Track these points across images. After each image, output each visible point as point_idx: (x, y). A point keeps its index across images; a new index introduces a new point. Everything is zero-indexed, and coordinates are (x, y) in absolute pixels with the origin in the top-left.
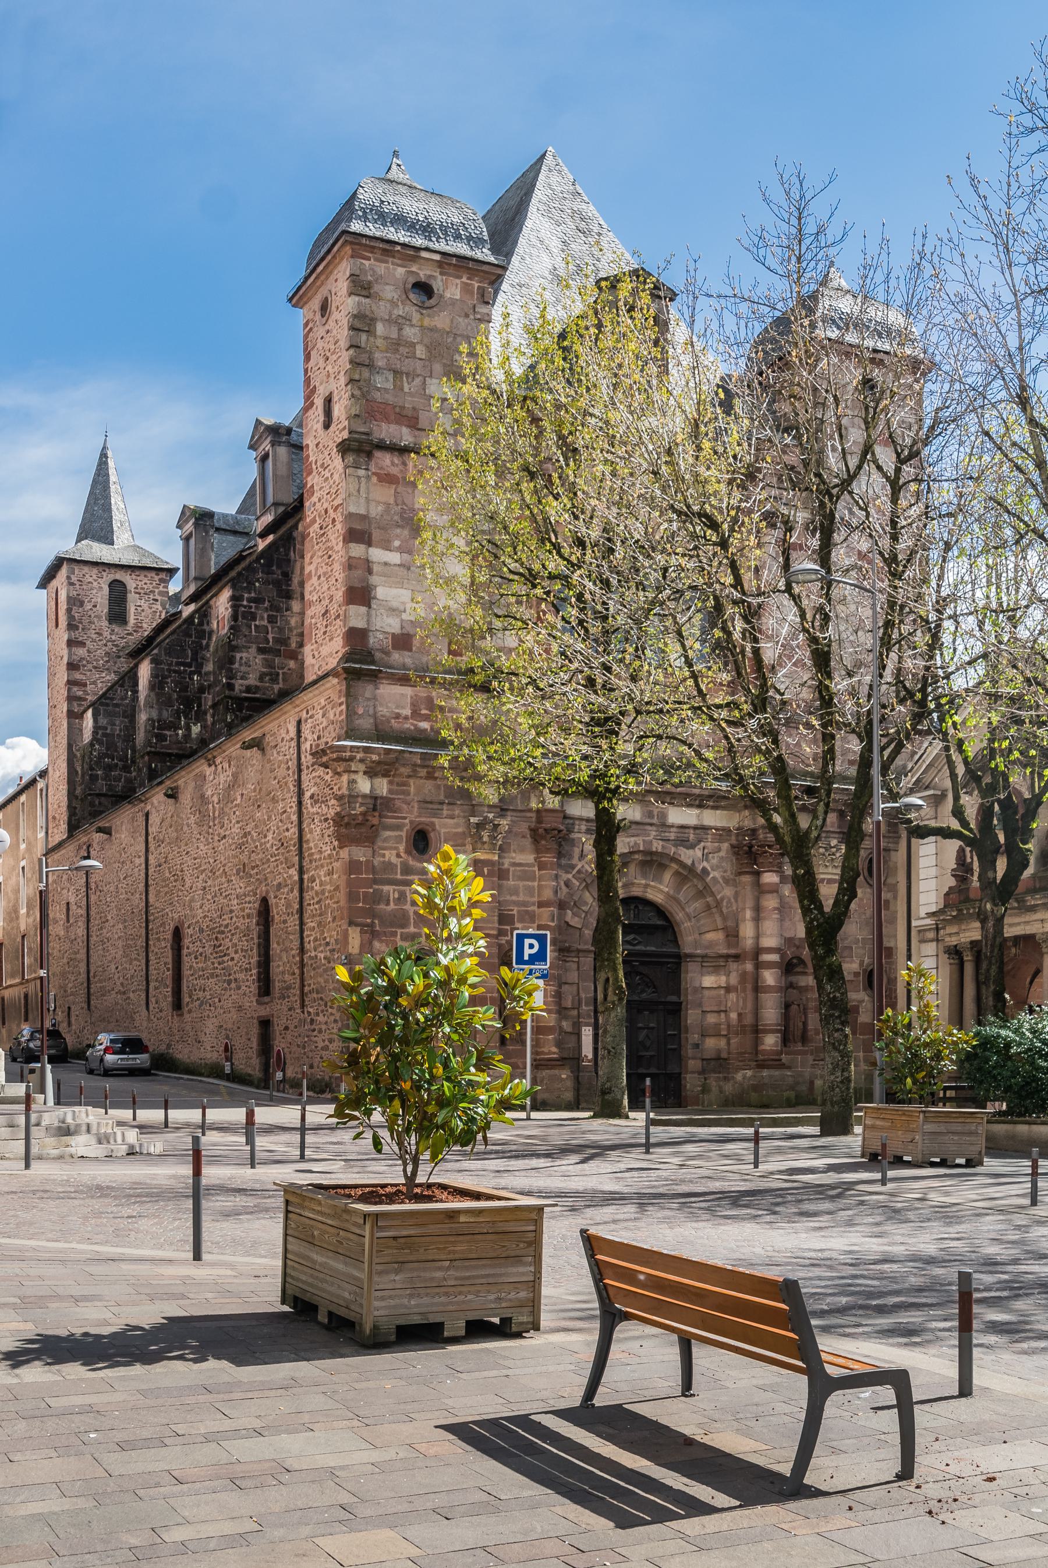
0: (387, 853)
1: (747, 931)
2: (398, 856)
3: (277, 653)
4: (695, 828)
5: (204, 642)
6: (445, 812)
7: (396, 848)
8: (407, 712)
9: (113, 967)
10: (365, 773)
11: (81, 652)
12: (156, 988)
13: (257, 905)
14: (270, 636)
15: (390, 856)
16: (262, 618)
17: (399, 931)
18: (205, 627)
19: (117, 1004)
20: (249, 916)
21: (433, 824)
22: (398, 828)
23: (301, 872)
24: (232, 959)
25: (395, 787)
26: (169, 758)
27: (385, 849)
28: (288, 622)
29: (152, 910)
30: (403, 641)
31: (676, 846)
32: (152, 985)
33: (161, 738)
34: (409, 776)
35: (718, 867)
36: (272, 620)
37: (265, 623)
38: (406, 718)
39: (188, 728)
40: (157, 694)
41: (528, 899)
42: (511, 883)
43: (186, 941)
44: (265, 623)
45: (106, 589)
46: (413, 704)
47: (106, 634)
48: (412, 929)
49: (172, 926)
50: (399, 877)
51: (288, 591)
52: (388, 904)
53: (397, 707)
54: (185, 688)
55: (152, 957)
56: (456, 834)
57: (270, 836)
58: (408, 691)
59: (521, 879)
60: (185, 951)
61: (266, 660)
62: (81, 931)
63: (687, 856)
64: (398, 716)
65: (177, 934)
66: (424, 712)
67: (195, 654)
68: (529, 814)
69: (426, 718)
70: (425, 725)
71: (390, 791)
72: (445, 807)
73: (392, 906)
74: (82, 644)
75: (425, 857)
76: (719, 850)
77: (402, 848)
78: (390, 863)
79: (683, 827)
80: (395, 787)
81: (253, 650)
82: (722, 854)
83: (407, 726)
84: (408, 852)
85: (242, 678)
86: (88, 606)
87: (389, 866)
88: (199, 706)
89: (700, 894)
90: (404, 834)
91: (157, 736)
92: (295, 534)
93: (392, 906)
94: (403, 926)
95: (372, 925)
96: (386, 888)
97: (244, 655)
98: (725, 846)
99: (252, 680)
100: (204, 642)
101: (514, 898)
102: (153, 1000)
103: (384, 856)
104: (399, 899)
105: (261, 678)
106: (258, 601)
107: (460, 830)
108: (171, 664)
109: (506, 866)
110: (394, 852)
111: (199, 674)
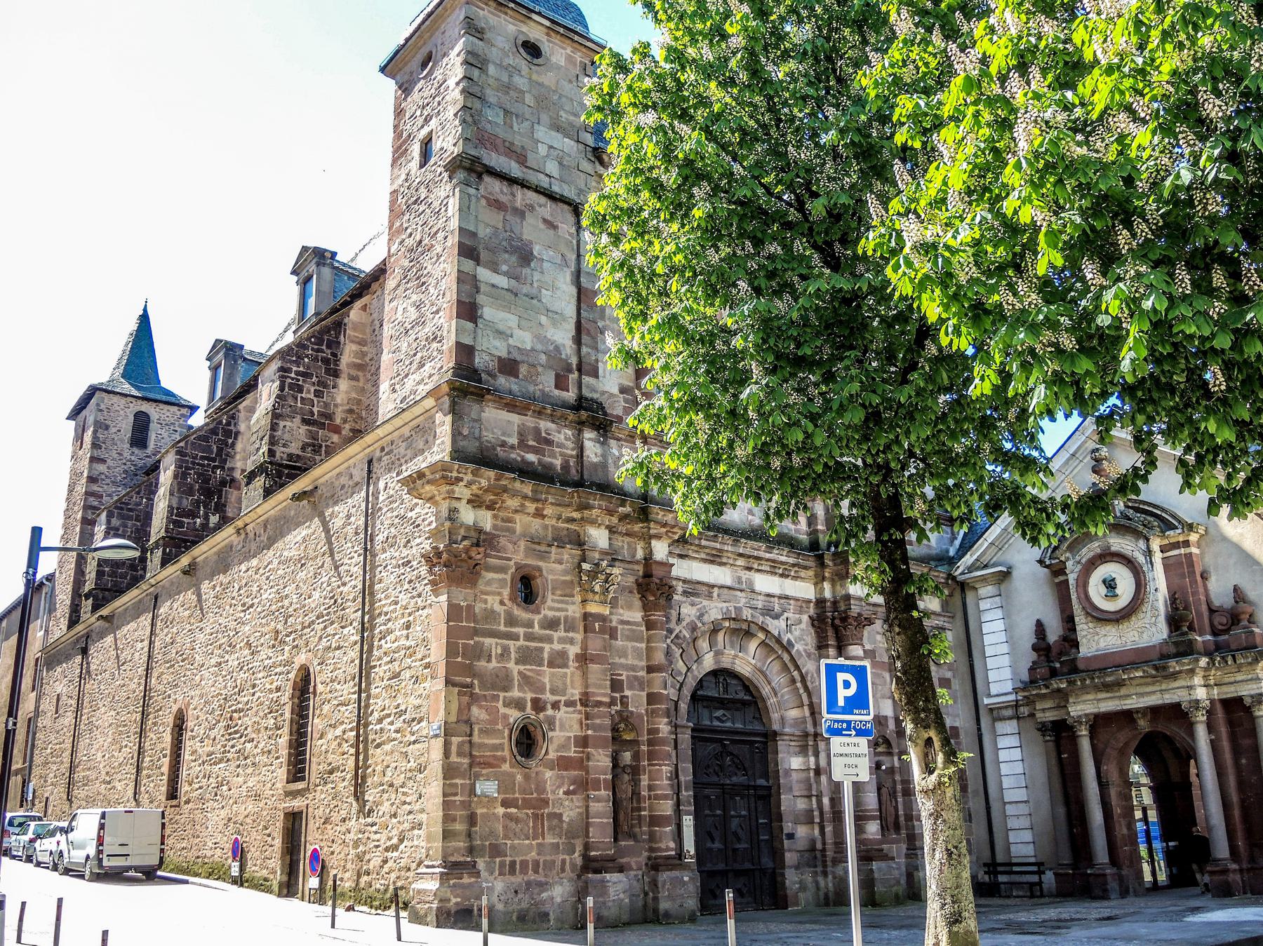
0: (489, 598)
4: (780, 597)
7: (499, 594)
8: (513, 440)
9: (100, 754)
11: (101, 468)
14: (315, 410)
15: (493, 602)
16: (309, 392)
17: (502, 695)
18: (232, 428)
20: (278, 689)
22: (502, 570)
25: (499, 523)
27: (487, 593)
28: (333, 398)
30: (509, 366)
31: (763, 615)
33: (178, 524)
34: (516, 511)
35: (801, 639)
36: (318, 394)
37: (312, 396)
38: (512, 447)
39: (207, 518)
40: (179, 483)
41: (636, 662)
42: (619, 643)
43: (190, 724)
44: (312, 396)
45: (131, 418)
46: (520, 434)
47: (127, 454)
48: (516, 693)
49: (175, 708)
50: (502, 628)
51: (336, 371)
52: (489, 661)
53: (504, 434)
54: (206, 481)
56: (564, 582)
57: (316, 595)
58: (515, 418)
59: (629, 639)
61: (310, 431)
62: (68, 719)
63: (776, 626)
64: (503, 444)
66: (531, 443)
67: (220, 450)
68: (636, 567)
69: (535, 451)
70: (531, 457)
71: (495, 527)
72: (553, 549)
73: (494, 664)
74: (103, 461)
75: (532, 607)
76: (800, 622)
77: (506, 592)
78: (493, 611)
79: (768, 595)
80: (499, 523)
81: (298, 419)
82: (803, 626)
84: (513, 599)
85: (284, 446)
87: (490, 615)
88: (220, 497)
90: (508, 577)
91: (175, 522)
92: (346, 321)
93: (494, 664)
94: (505, 689)
95: (471, 686)
96: (488, 641)
97: (288, 424)
98: (805, 618)
99: (294, 449)
101: (623, 661)
103: (486, 602)
104: (502, 655)
105: (303, 448)
106: (306, 375)
107: (568, 578)
108: (195, 458)
109: (614, 624)
110: (498, 598)
111: (223, 468)
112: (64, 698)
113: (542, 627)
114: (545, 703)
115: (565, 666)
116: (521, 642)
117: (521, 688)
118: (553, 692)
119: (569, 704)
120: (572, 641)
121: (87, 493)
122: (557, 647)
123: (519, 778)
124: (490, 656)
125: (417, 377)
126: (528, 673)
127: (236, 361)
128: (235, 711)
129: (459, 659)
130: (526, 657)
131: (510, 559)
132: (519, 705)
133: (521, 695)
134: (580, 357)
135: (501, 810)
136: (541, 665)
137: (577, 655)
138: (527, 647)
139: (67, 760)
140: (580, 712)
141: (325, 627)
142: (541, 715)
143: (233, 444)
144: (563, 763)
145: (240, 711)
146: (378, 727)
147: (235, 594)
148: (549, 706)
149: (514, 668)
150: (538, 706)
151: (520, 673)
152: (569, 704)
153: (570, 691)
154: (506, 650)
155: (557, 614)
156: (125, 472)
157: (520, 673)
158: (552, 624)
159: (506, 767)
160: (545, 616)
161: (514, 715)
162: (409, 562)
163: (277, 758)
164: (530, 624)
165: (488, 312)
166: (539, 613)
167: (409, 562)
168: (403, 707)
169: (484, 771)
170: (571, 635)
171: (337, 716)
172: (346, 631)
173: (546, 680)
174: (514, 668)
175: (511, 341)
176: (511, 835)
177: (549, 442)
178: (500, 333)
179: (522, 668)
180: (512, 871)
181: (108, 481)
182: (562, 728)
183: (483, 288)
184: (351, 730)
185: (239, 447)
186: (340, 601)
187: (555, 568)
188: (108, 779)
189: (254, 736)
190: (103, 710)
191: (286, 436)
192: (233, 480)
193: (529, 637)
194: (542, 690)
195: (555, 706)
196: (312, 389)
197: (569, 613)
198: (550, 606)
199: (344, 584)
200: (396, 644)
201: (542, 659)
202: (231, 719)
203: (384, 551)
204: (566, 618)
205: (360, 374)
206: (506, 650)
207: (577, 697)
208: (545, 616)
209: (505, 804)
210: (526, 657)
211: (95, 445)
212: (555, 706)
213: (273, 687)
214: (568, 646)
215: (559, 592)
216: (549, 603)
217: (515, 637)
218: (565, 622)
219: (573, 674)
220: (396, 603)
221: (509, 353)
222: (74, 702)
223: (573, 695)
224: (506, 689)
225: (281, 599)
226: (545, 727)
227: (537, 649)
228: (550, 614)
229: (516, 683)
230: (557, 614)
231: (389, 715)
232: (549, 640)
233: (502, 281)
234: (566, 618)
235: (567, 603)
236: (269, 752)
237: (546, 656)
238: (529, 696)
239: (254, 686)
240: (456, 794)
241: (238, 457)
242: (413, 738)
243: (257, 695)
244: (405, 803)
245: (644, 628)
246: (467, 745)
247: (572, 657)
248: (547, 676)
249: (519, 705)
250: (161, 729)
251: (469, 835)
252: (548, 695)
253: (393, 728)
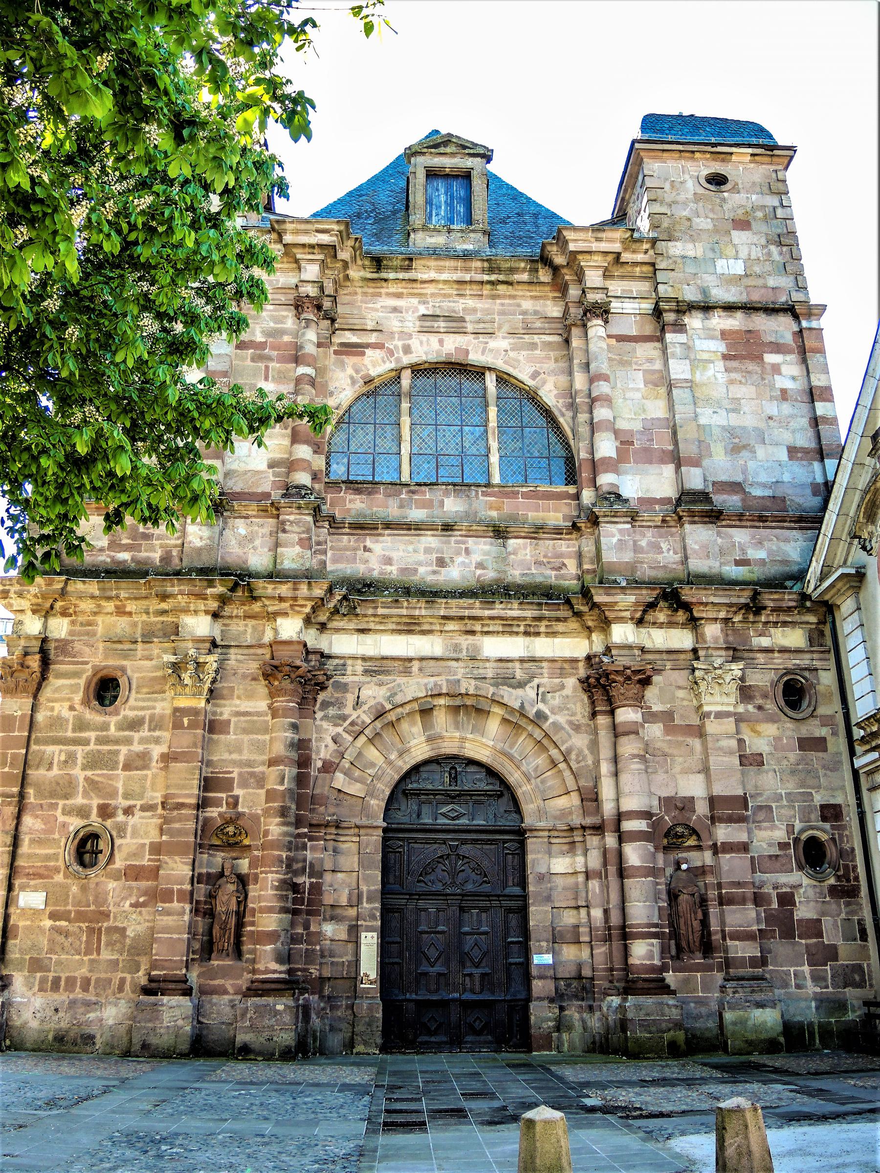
6: (139, 653)
17: (61, 803)
21: (123, 670)
48: (79, 800)
72: (140, 646)
94: (66, 797)
104: (66, 762)
114: (116, 808)
116: (92, 747)
117: (86, 794)
118: (126, 796)
123: (75, 889)
126: (97, 779)
132: (82, 812)
133: (85, 801)
135: (48, 923)
138: (99, 751)
142: (109, 823)
148: (120, 812)
150: (105, 812)
151: (86, 779)
158: (134, 725)
159: (59, 878)
160: (125, 717)
161: (75, 823)
164: (105, 727)
166: (118, 714)
169: (32, 883)
170: (157, 733)
173: (120, 785)
176: (58, 949)
179: (89, 773)
180: (56, 985)
182: (135, 834)
187: (140, 667)
194: (113, 794)
195: (128, 811)
198: (132, 704)
201: (117, 763)
209: (53, 916)
214: (152, 746)
216: (132, 702)
218: (150, 722)
219: (155, 776)
227: (110, 752)
228: (131, 714)
229: (81, 789)
232: (128, 741)
235: (155, 700)
237: (121, 758)
238: (95, 802)
248: (120, 780)
252: (120, 800)
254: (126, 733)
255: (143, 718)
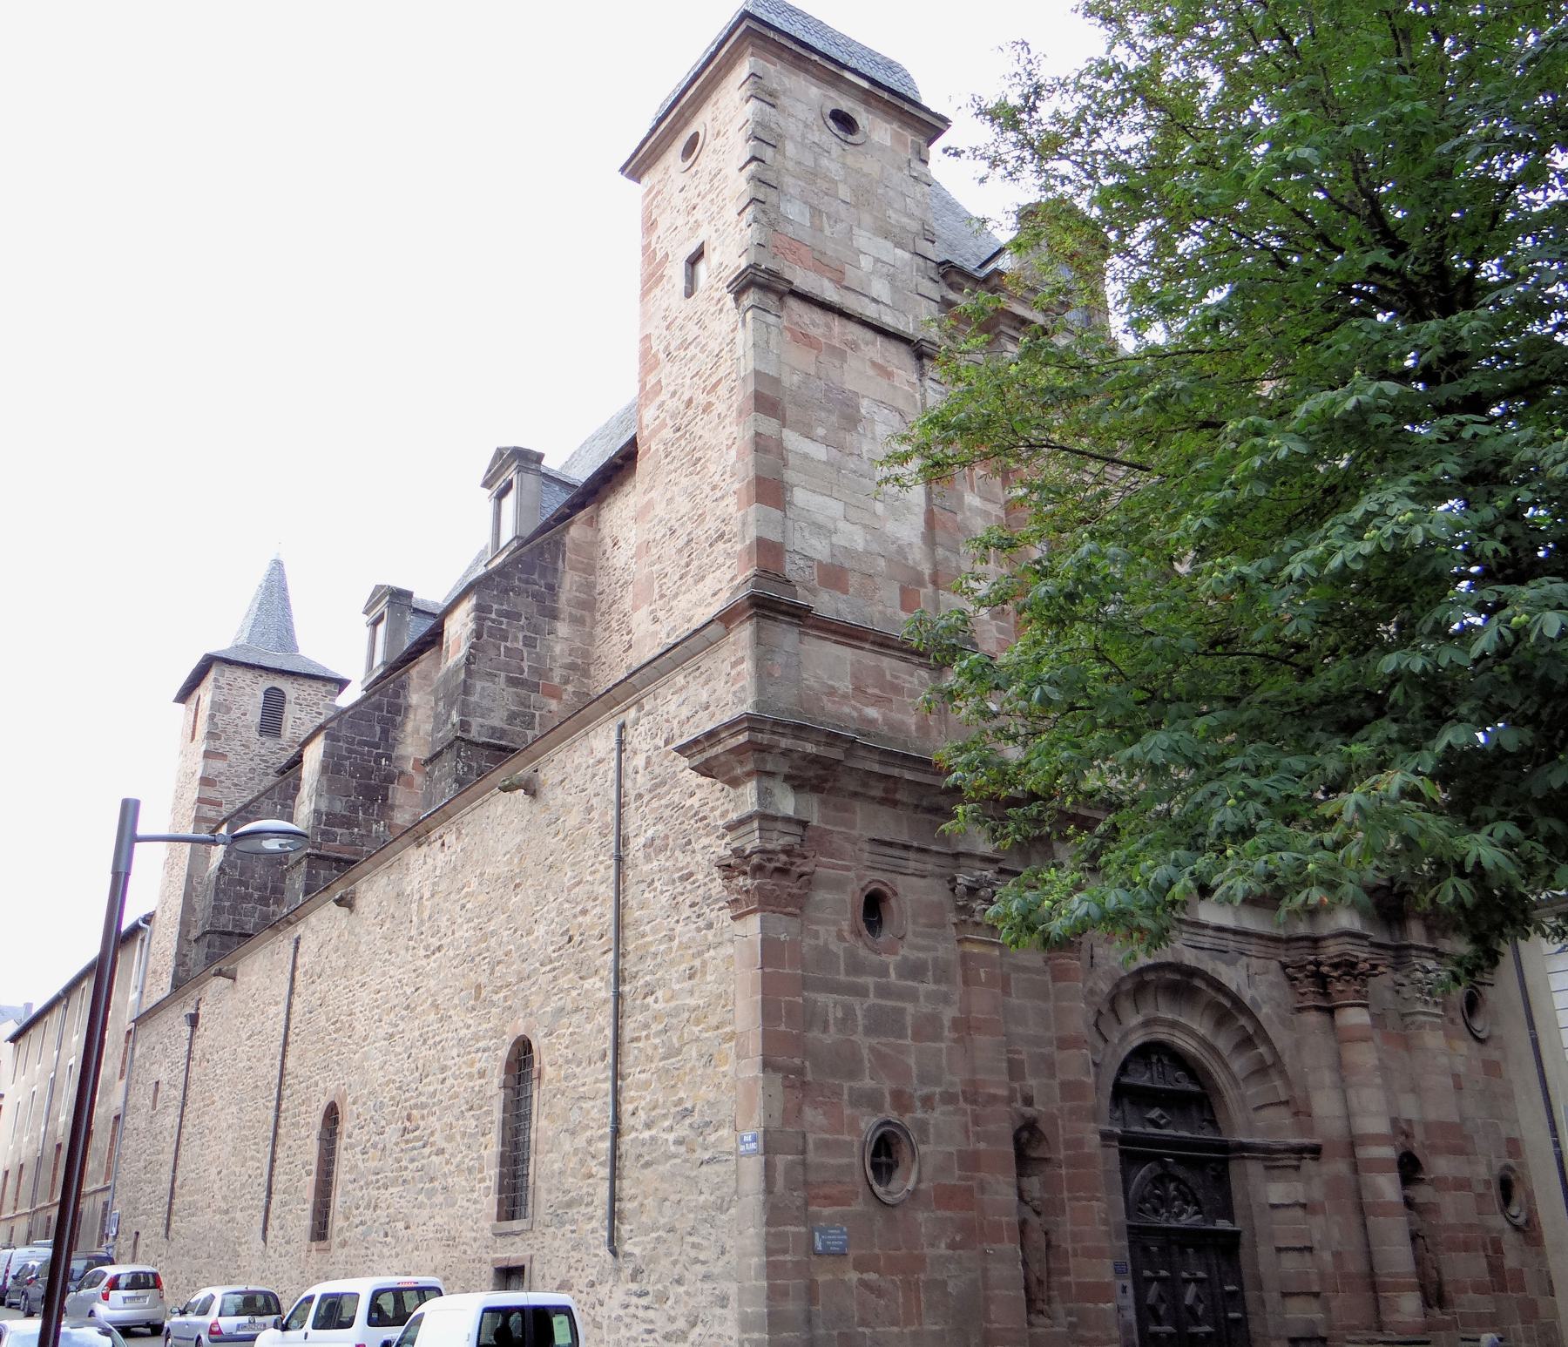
0: (821, 929)
1: (1325, 1105)
2: (840, 937)
3: (535, 687)
5: (399, 719)
7: (835, 923)
8: (845, 686)
9: (214, 1171)
10: (788, 778)
11: (219, 765)
12: (284, 1204)
13: (504, 1053)
14: (525, 665)
17: (846, 1085)
18: (401, 701)
19: (212, 1228)
20: (482, 1074)
23: (619, 978)
24: (441, 1152)
26: (334, 865)
27: (818, 923)
28: (550, 648)
29: (288, 1080)
30: (833, 576)
32: (276, 1198)
36: (529, 643)
37: (520, 645)
38: (845, 696)
43: (346, 1126)
44: (520, 645)
46: (855, 676)
47: (255, 747)
48: (868, 1083)
50: (842, 977)
52: (825, 1029)
53: (830, 678)
55: (280, 1154)
57: (540, 930)
60: (342, 1142)
62: (171, 1119)
64: (832, 692)
65: (332, 1115)
67: (385, 732)
69: (878, 701)
70: (872, 712)
74: (223, 756)
83: (846, 710)
85: (482, 716)
86: (235, 714)
87: (824, 955)
88: (385, 798)
89: (1246, 1042)
91: (324, 833)
95: (800, 1071)
96: (823, 998)
99: (497, 720)
100: (399, 719)
101: (1020, 1030)
102: (274, 1223)
103: (816, 935)
106: (512, 616)
107: (935, 898)
110: (833, 929)
111: (389, 758)
112: (163, 1087)
113: (900, 976)
115: (937, 1037)
116: (873, 1000)
118: (924, 1079)
119: (949, 1098)
120: (946, 999)
121: (200, 800)
122: (926, 1008)
124: (826, 1022)
125: (693, 596)
126: (883, 1049)
127: (403, 613)
128: (416, 1106)
129: (783, 1028)
130: (882, 1023)
131: (848, 869)
132: (871, 1101)
134: (935, 564)
136: (902, 1036)
137: (955, 1021)
139: (166, 1176)
140: (965, 1113)
141: (555, 978)
143: (403, 724)
144: (946, 1197)
145: (423, 1106)
146: (646, 1134)
147: (414, 932)
149: (865, 1043)
151: (872, 1049)
152: (949, 1098)
153: (948, 1077)
154: (849, 1012)
155: (921, 955)
156: (253, 770)
157: (872, 1049)
158: (914, 970)
160: (905, 959)
162: (691, 874)
163: (482, 1180)
164: (883, 971)
165: (800, 496)
166: (896, 953)
167: (691, 874)
168: (688, 1105)
171: (575, 1116)
172: (588, 984)
173: (912, 1061)
174: (865, 1043)
175: (834, 539)
177: (897, 689)
178: (819, 529)
179: (874, 1041)
181: (228, 783)
183: (791, 459)
184: (602, 1138)
185: (409, 727)
186: (577, 939)
188: (224, 1206)
189: (444, 1145)
190: (219, 1105)
191: (486, 703)
192: (402, 773)
193: (884, 991)
195: (927, 1102)
196: (521, 637)
197: (940, 954)
199: (584, 912)
200: (673, 1004)
201: (904, 1027)
202: (409, 1118)
203: (648, 859)
204: (936, 960)
205: (586, 613)
206: (849, 1012)
207: (958, 1089)
208: (905, 959)
210: (882, 1023)
211: (212, 735)
212: (927, 1102)
213: (474, 1070)
215: (922, 921)
216: (910, 937)
217: (860, 992)
220: (671, 939)
221: (833, 555)
222: (178, 1094)
223: (952, 1084)
224: (853, 1074)
225: (484, 938)
226: (914, 1136)
228: (914, 955)
230: (921, 955)
231: (665, 1116)
232: (912, 996)
233: (819, 452)
234: (936, 960)
236: (470, 1170)
237: (909, 1020)
238: (887, 1086)
239: (443, 1069)
240: (785, 1252)
241: (409, 741)
242: (706, 1156)
243: (448, 1083)
244: (697, 1261)
245: (1048, 978)
246: (800, 1169)
247: (947, 1023)
249: (871, 1101)
250: (304, 1133)
251: (809, 1321)
253: (671, 1137)
254: (910, 983)
255: (926, 962)
